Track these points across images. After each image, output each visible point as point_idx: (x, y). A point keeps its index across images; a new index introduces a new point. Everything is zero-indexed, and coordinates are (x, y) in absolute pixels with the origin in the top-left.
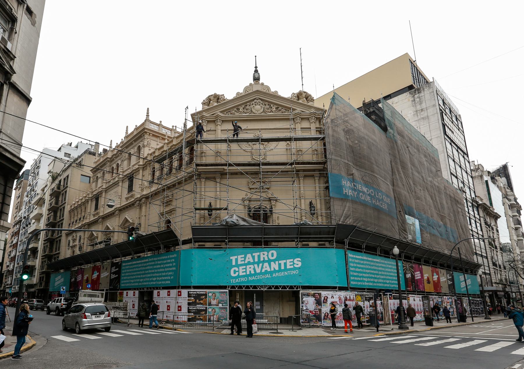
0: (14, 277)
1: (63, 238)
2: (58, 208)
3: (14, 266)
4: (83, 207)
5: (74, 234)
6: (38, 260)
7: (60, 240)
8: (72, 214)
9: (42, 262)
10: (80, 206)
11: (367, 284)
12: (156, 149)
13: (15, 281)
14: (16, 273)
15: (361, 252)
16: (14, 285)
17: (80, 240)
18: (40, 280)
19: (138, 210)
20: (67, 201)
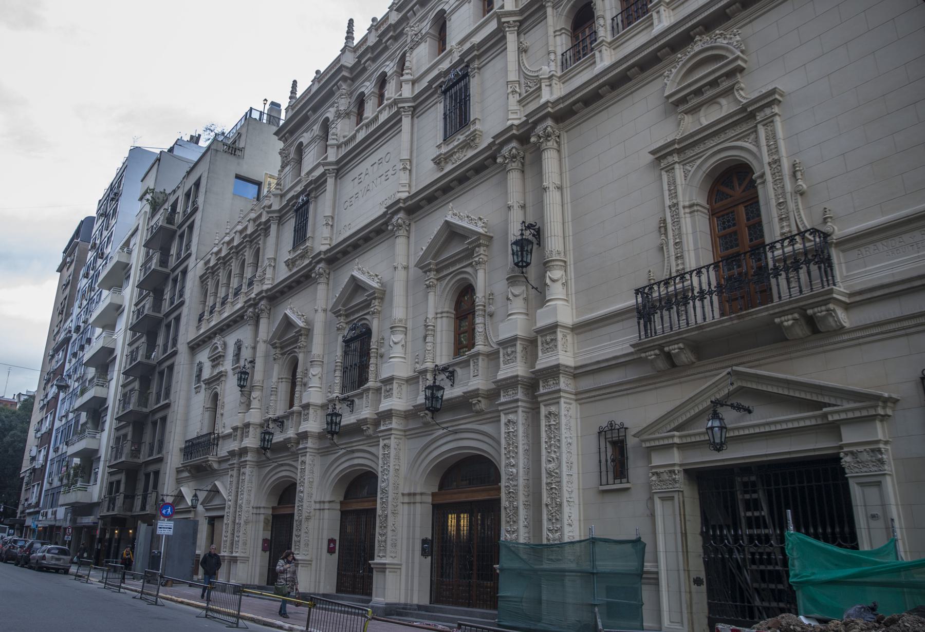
0: (46, 486)
1: (182, 360)
2: (160, 321)
3: (47, 456)
4: (248, 255)
5: (218, 341)
6: (105, 435)
8: (210, 284)
9: (118, 439)
10: (237, 251)
13: (46, 496)
14: (50, 474)
16: (45, 507)
17: (237, 356)
18: (110, 492)
20: (194, 249)
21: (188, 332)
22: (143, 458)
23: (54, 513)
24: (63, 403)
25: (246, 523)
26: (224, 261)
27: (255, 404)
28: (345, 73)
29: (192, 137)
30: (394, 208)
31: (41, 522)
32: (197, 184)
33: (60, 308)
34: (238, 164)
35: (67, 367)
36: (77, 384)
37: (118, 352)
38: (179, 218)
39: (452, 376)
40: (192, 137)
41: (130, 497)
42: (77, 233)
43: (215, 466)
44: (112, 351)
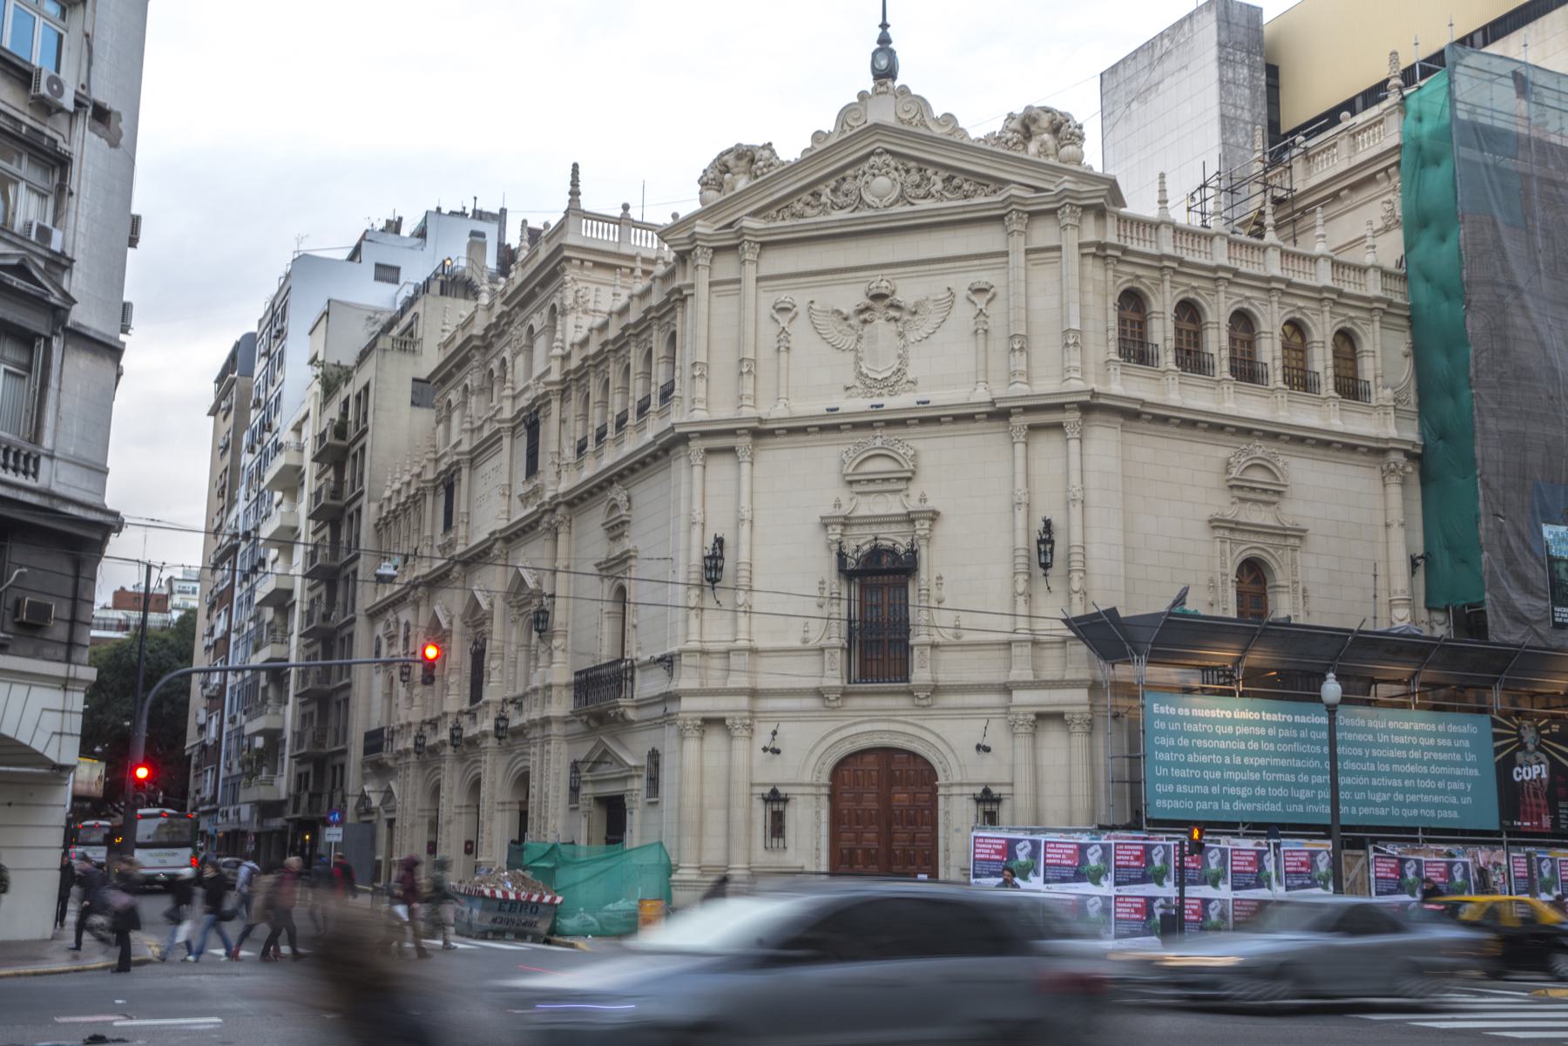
0: (223, 773)
1: (361, 629)
7: (351, 636)
11: (1249, 807)
12: (610, 314)
13: (225, 786)
15: (1231, 693)
16: (223, 804)
18: (299, 788)
19: (549, 545)
21: (367, 597)
22: (330, 748)
23: (237, 813)
24: (236, 648)
25: (412, 826)
26: (394, 515)
27: (417, 701)
28: (476, 343)
29: (389, 222)
30: (493, 538)
31: (222, 825)
32: (366, 388)
33: (220, 485)
34: (415, 364)
35: (237, 592)
36: (252, 625)
37: (297, 596)
38: (352, 433)
39: (520, 707)
40: (389, 222)
41: (315, 796)
42: (233, 357)
43: (391, 763)
44: (290, 592)
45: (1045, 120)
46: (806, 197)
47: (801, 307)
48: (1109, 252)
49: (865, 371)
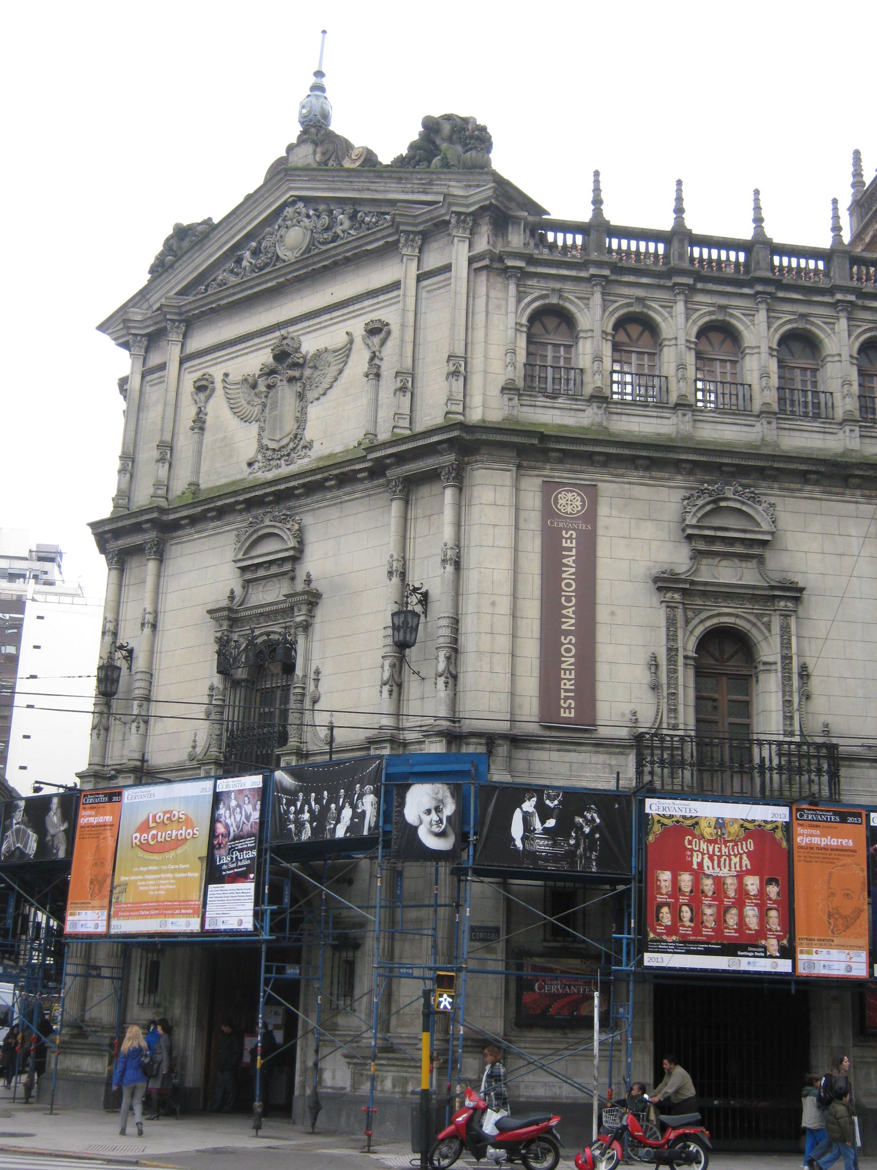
45: (447, 128)
46: (231, 265)
47: (218, 378)
48: (510, 263)
49: (265, 442)
